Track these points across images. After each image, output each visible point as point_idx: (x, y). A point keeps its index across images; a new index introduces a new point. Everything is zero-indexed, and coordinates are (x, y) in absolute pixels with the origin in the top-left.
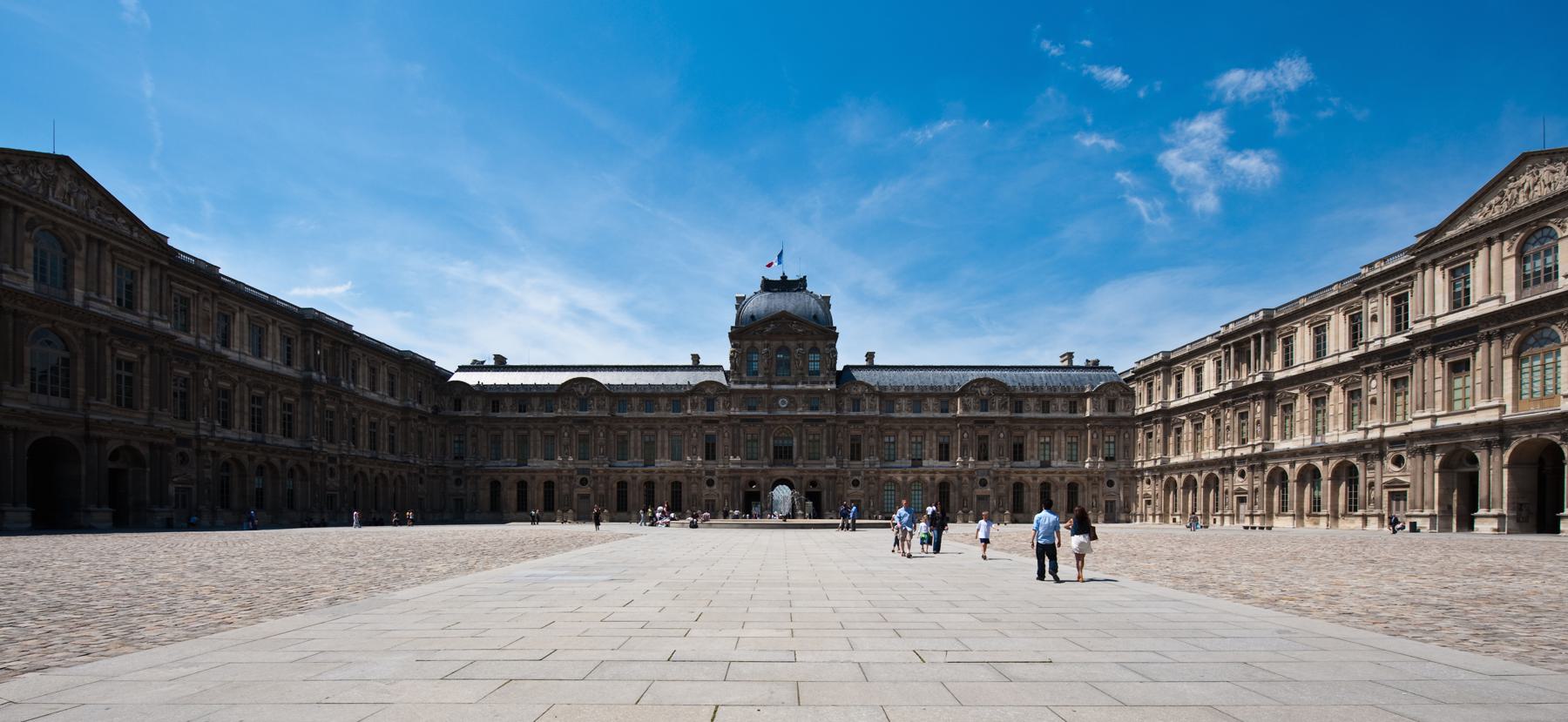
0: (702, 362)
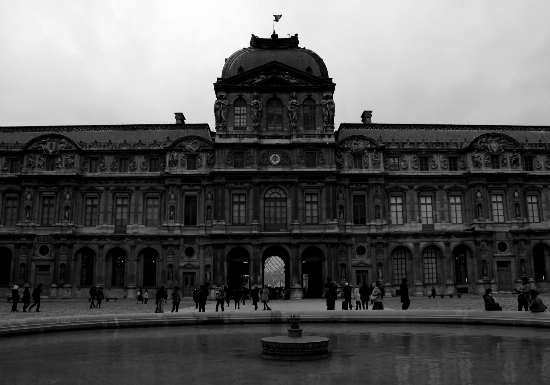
0: (186, 122)
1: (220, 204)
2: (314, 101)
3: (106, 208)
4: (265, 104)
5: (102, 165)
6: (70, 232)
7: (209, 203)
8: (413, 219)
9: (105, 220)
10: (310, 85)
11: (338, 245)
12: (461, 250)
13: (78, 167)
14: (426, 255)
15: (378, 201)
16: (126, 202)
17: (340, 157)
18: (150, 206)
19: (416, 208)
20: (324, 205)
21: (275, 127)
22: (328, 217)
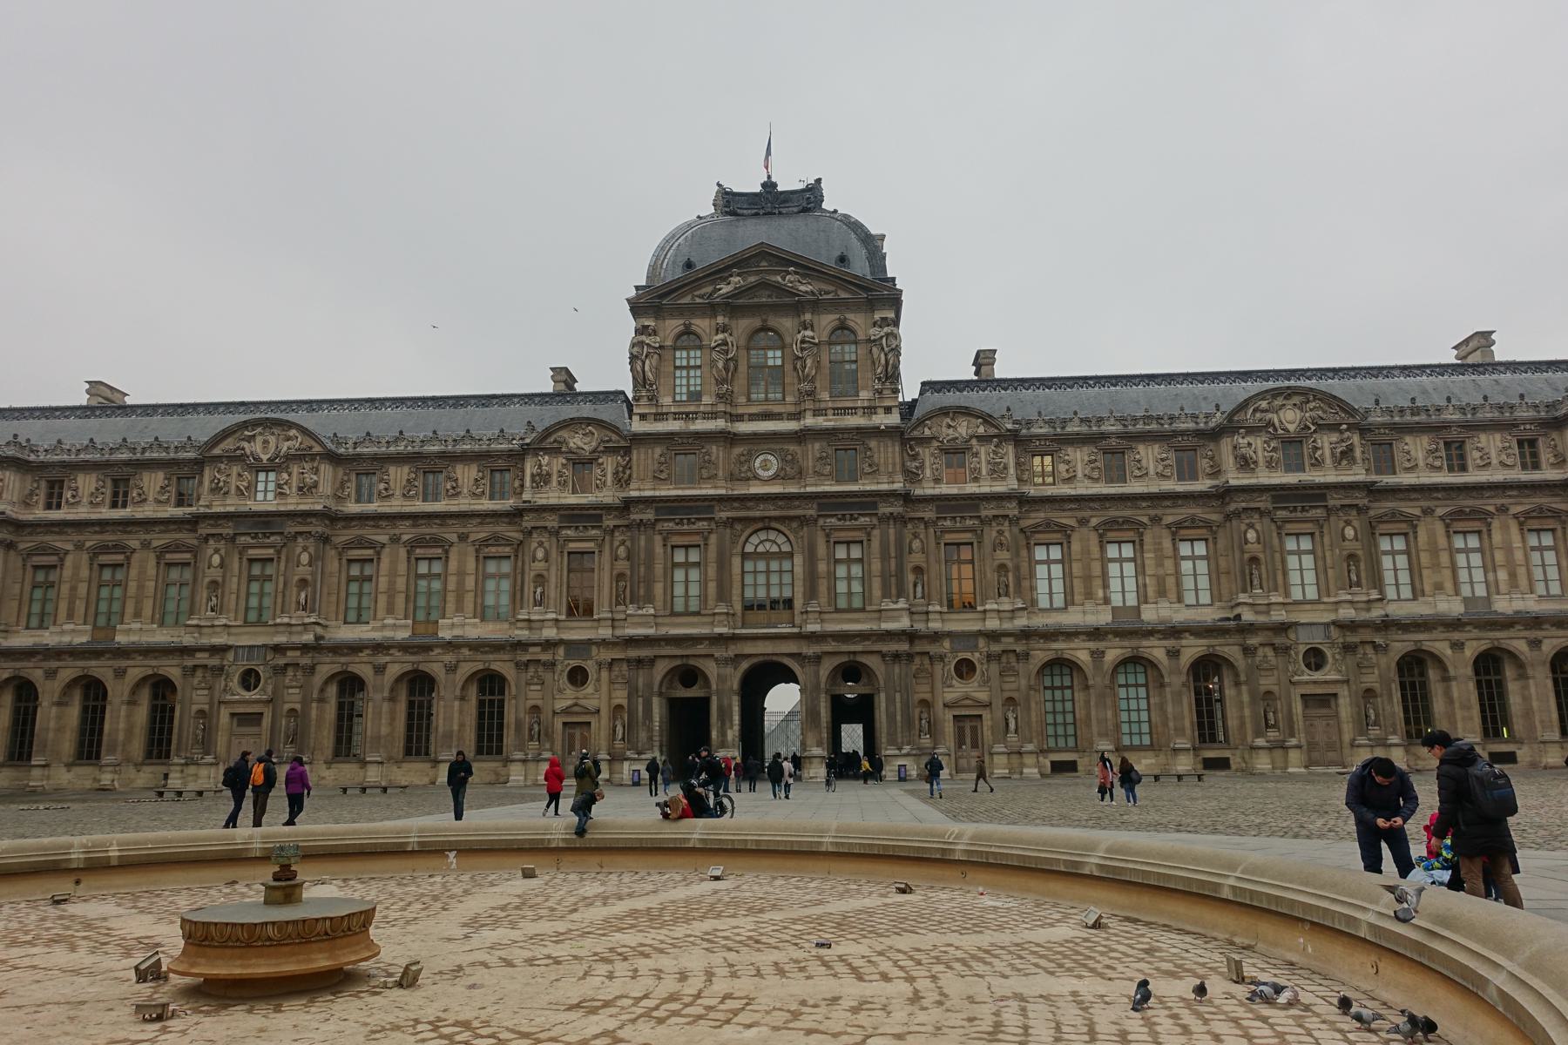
0: (578, 387)
1: (642, 569)
2: (853, 332)
3: (392, 583)
4: (742, 342)
5: (382, 486)
6: (308, 638)
7: (622, 566)
8: (1089, 595)
9: (390, 610)
10: (843, 295)
11: (910, 657)
12: (1206, 667)
13: (329, 491)
14: (1121, 680)
15: (1003, 556)
16: (437, 568)
17: (915, 457)
18: (493, 576)
19: (1096, 568)
20: (876, 566)
21: (766, 393)
22: (886, 594)
